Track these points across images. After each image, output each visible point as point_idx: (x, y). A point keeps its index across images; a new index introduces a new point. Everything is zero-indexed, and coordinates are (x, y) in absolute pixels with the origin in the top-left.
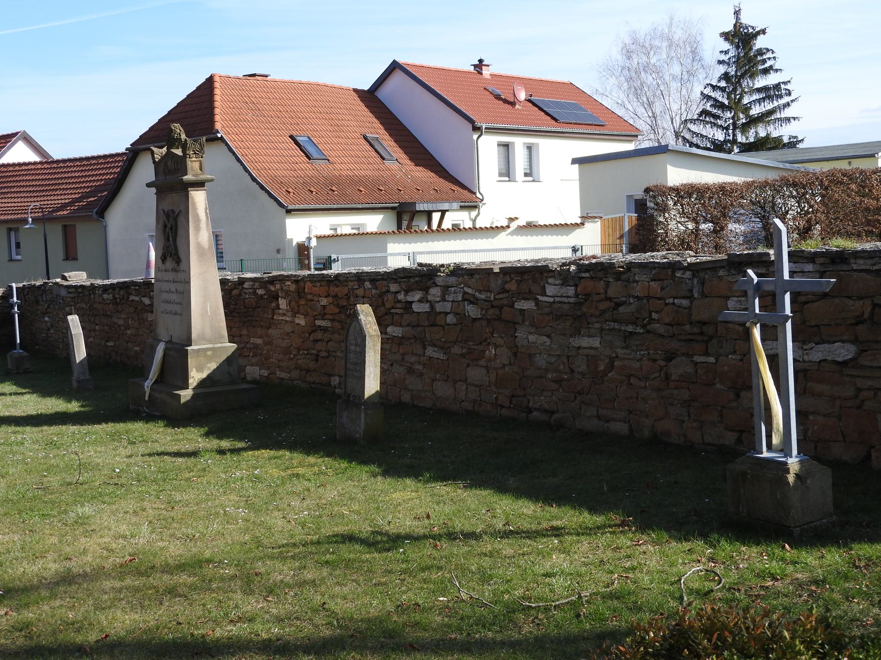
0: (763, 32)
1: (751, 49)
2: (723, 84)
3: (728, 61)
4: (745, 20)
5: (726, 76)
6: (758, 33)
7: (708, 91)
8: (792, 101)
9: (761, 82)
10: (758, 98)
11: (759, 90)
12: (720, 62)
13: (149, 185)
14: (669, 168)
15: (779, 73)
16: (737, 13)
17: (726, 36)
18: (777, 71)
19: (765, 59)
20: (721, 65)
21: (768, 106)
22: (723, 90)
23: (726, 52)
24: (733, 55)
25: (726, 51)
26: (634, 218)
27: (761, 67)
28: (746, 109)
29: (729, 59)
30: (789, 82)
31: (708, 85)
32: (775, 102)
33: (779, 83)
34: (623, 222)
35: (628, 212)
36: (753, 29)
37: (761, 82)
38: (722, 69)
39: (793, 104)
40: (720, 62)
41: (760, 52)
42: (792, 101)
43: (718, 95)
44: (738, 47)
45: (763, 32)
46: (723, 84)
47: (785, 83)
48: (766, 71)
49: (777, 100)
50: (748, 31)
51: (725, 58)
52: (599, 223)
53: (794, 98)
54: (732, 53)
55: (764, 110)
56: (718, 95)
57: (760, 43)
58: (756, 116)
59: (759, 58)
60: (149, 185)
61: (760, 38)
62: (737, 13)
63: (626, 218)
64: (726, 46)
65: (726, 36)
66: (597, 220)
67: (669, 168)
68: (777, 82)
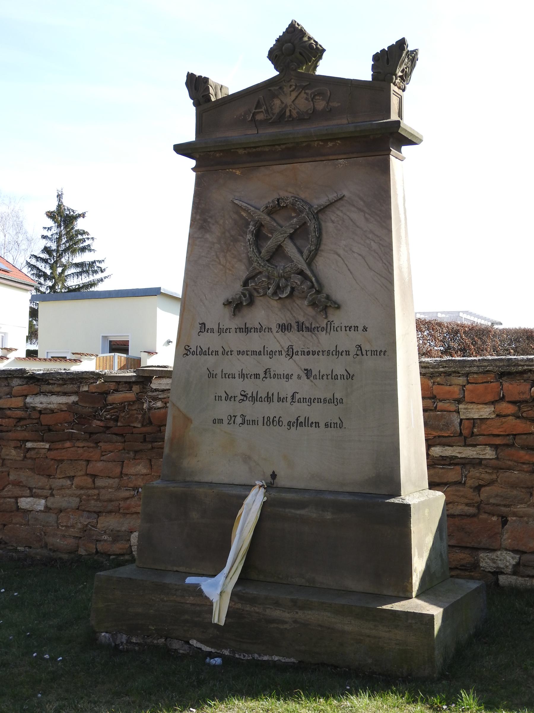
0: (83, 215)
1: (73, 228)
2: (45, 256)
3: (51, 237)
4: (67, 203)
5: (47, 250)
6: (79, 216)
7: (33, 262)
8: (105, 278)
9: (79, 258)
10: (76, 272)
11: (77, 265)
12: (44, 237)
13: (181, 149)
14: (159, 311)
15: (92, 252)
16: (59, 196)
17: (51, 215)
18: (90, 250)
19: (84, 239)
20: (44, 240)
21: (85, 279)
22: (45, 261)
23: (49, 229)
24: (56, 232)
25: (49, 228)
26: (123, 358)
27: (81, 245)
28: (62, 278)
29: (52, 235)
30: (103, 261)
31: (32, 255)
32: (91, 276)
33: (95, 261)
34: (113, 361)
35: (103, 352)
36: (73, 212)
37: (79, 258)
38: (44, 243)
39: (106, 281)
40: (44, 237)
41: (79, 232)
42: (105, 278)
43: (41, 265)
44: (59, 226)
45: (83, 215)
46: (45, 256)
47: (100, 262)
48: (83, 249)
49: (93, 275)
50: (70, 213)
51: (49, 234)
52: (95, 360)
53: (107, 276)
54: (55, 230)
55: (81, 282)
56: (41, 265)
57: (80, 225)
58: (74, 287)
59: (80, 237)
60: (181, 149)
61: (80, 220)
62: (59, 196)
63: (116, 357)
64: (50, 223)
65: (51, 215)
66: (93, 357)
67: (159, 311)
68: (93, 260)
